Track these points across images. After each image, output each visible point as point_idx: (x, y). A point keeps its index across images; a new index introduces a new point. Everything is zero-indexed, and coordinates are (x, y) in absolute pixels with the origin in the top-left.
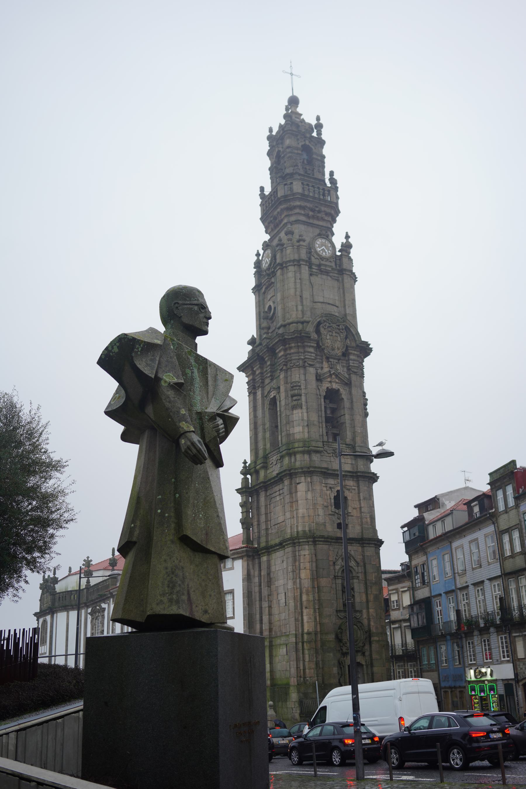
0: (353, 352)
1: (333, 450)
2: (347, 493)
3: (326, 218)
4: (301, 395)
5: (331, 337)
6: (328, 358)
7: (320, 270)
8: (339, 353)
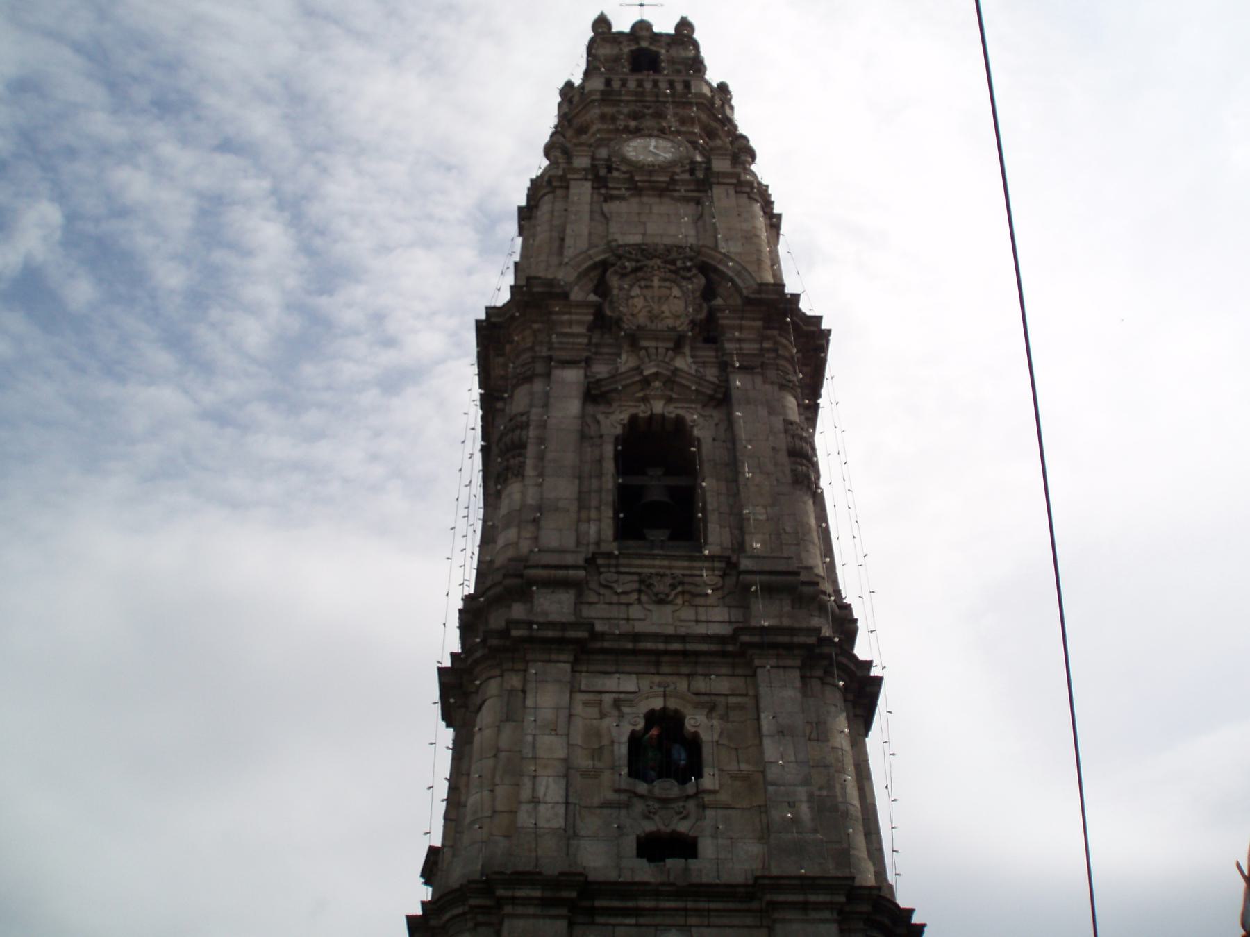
0: (737, 322)
1: (641, 582)
2: (696, 721)
3: (683, 129)
4: (522, 446)
5: (648, 293)
6: (633, 341)
8: (683, 326)
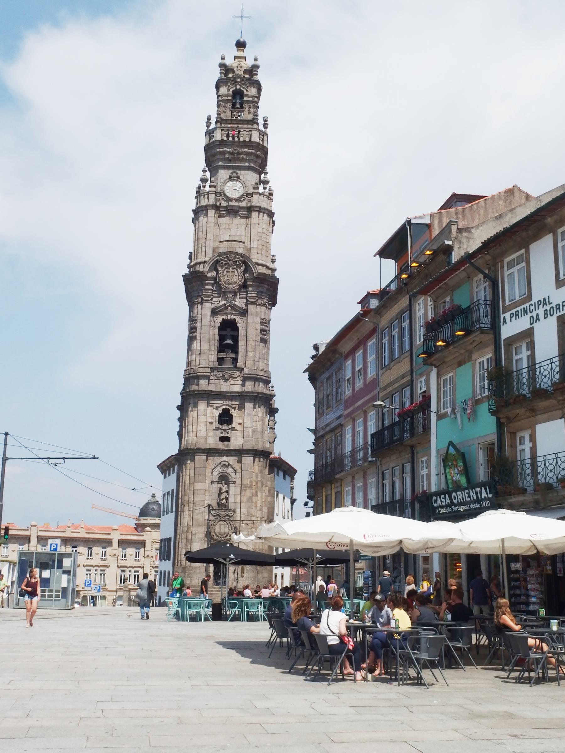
2: (232, 411)
4: (196, 328)
5: (228, 274)
7: (227, 210)
